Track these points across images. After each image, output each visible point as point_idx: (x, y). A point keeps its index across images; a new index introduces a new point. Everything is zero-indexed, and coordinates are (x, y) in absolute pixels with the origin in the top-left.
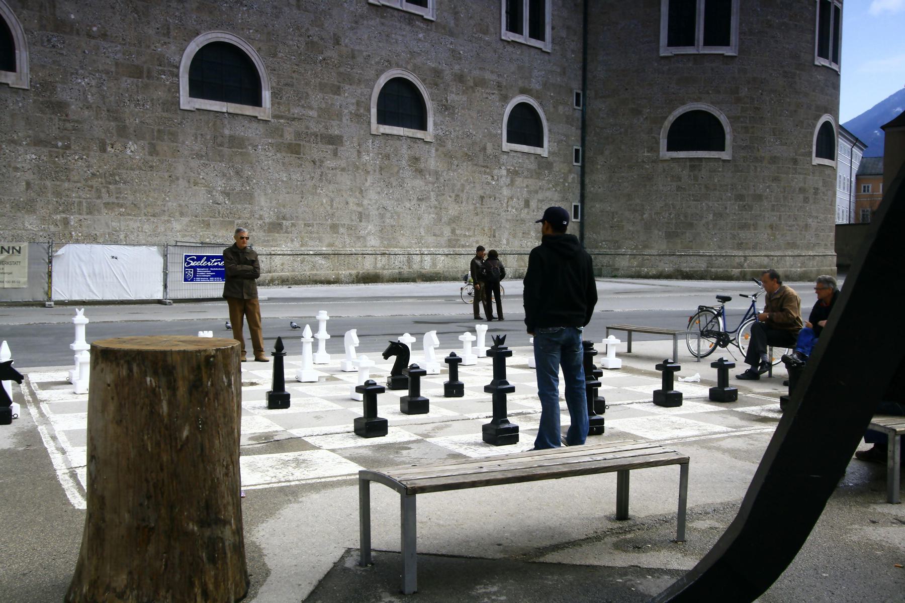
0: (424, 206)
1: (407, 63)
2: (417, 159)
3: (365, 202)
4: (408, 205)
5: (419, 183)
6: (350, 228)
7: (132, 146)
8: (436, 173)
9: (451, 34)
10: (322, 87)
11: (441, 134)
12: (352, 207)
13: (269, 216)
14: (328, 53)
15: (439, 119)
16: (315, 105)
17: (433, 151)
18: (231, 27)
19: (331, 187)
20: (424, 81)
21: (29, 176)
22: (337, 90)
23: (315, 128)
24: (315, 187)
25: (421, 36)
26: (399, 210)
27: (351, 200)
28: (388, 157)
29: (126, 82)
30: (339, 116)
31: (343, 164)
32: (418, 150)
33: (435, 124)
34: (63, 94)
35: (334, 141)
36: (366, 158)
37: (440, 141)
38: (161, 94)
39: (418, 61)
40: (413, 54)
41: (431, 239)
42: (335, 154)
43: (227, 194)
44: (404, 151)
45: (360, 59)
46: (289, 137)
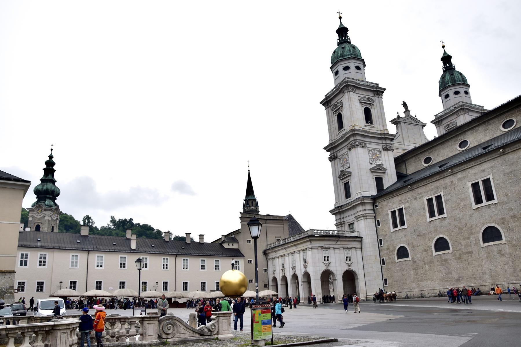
0: (507, 266)
1: (490, 220)
2: (500, 251)
3: (484, 269)
4: (500, 267)
5: (503, 259)
6: (480, 278)
7: (427, 266)
8: (510, 253)
9: (506, 203)
10: (464, 239)
11: (509, 239)
12: (479, 271)
13: (456, 277)
14: (464, 229)
15: (507, 234)
16: (463, 244)
17: (507, 246)
18: (441, 233)
19: (472, 266)
20: (498, 224)
21: (413, 276)
22: (469, 238)
23: (464, 251)
24: (467, 267)
25: (494, 210)
26: (497, 269)
27: (479, 269)
28: (489, 253)
29: (424, 253)
30: (470, 245)
31: (474, 259)
32: (500, 247)
33: (505, 237)
34: (416, 259)
35: (470, 253)
36: (481, 255)
37: (509, 242)
38: (430, 254)
39: (494, 218)
40: (492, 217)
41: (513, 278)
42: (471, 256)
43: (446, 273)
44: (495, 249)
45: (474, 227)
46: (458, 255)
